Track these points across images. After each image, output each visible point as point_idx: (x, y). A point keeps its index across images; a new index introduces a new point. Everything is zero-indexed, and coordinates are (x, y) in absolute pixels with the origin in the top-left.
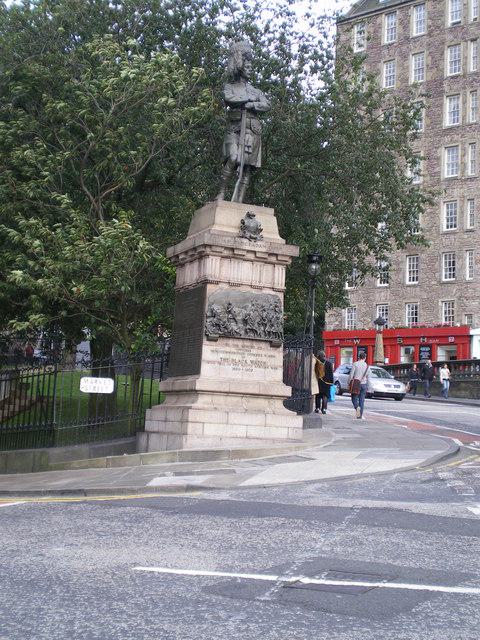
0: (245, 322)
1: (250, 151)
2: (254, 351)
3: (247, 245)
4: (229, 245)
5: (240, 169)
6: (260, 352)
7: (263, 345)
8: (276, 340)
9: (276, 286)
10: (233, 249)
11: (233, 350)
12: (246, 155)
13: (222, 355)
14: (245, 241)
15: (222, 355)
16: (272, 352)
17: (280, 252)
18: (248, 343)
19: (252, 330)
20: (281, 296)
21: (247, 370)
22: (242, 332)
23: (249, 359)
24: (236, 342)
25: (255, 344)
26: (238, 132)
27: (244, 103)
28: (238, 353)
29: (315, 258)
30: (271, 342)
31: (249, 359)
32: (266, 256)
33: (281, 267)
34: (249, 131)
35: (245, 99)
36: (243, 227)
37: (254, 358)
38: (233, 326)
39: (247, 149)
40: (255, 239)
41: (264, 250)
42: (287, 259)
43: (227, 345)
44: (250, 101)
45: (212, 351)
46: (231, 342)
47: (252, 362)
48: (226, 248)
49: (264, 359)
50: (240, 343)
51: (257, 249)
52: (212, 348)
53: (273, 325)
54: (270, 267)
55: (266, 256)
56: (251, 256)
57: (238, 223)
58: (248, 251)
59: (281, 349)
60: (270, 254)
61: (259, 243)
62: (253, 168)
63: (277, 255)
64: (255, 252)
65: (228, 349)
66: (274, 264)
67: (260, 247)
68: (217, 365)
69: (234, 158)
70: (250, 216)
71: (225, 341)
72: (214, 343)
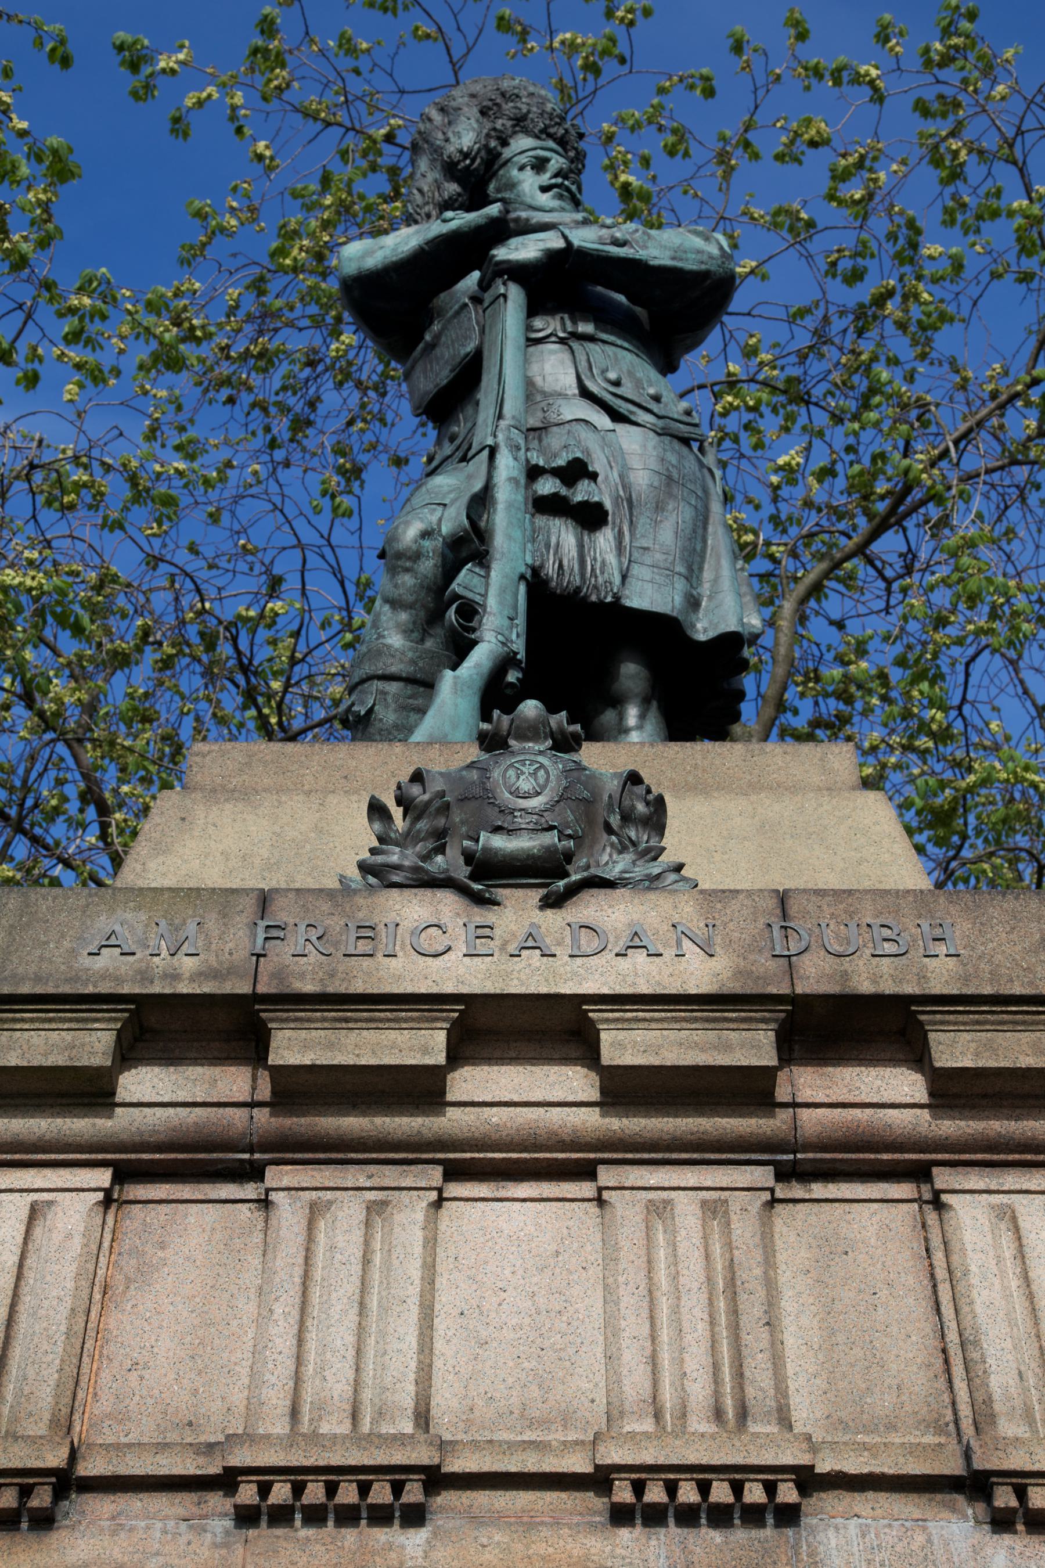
14: (412, 909)
17: (941, 975)
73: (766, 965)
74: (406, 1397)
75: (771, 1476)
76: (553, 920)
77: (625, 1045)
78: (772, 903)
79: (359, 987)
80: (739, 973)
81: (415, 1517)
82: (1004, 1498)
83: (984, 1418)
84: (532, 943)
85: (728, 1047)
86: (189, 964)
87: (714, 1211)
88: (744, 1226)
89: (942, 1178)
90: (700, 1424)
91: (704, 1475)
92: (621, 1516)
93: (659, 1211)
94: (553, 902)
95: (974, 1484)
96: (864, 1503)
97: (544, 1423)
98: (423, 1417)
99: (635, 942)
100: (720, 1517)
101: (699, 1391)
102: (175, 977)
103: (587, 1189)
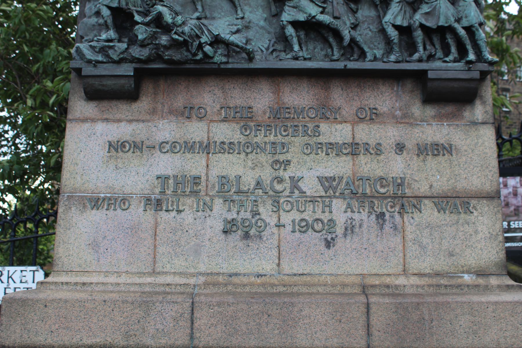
2: (338, 133)
6: (365, 133)
7: (384, 99)
8: (446, 68)
13: (166, 164)
15: (166, 164)
16: (436, 132)
18: (300, 97)
19: (310, 28)
21: (304, 227)
24: (239, 95)
28: (248, 148)
30: (419, 77)
31: (311, 171)
37: (339, 167)
43: (188, 113)
45: (117, 147)
46: (209, 96)
49: (396, 166)
50: (260, 98)
52: (122, 131)
65: (196, 131)
68: (137, 212)
71: (181, 96)
72: (123, 109)
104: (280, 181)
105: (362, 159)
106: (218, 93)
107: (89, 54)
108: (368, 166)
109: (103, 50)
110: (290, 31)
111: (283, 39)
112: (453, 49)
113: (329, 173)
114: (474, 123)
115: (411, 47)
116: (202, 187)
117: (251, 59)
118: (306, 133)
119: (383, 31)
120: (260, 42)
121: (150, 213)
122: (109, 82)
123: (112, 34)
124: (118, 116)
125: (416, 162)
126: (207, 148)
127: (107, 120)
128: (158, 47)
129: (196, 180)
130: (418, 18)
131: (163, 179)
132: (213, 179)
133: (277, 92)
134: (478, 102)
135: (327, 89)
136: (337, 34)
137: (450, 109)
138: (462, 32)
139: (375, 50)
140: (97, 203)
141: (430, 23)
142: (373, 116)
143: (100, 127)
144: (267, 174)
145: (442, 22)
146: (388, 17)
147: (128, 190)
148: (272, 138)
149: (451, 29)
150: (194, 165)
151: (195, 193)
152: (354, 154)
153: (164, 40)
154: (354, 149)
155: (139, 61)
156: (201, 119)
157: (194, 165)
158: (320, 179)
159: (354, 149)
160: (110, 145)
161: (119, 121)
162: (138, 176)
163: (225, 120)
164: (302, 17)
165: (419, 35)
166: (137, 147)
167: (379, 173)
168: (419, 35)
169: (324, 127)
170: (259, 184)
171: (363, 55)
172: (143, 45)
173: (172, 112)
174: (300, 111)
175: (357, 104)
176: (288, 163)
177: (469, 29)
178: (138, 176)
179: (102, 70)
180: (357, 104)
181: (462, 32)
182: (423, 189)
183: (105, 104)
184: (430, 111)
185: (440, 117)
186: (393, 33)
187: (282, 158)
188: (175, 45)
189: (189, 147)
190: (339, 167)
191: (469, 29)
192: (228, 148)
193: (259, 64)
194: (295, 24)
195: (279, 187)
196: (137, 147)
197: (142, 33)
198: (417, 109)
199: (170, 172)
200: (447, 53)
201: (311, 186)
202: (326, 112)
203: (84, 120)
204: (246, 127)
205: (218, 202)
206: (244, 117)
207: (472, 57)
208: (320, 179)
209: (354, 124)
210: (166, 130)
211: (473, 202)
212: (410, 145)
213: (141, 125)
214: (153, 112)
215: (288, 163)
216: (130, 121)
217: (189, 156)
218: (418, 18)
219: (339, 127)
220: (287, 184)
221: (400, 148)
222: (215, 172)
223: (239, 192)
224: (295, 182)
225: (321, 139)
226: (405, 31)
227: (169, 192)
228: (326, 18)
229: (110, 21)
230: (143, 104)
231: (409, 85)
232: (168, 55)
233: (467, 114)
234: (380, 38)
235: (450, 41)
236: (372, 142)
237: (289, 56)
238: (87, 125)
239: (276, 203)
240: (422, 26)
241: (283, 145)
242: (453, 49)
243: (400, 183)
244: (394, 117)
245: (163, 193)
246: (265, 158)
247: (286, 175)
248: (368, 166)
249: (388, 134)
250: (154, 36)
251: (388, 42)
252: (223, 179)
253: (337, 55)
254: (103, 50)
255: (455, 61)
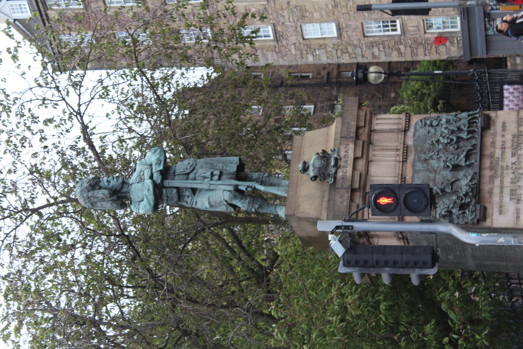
0: (456, 167)
1: (217, 172)
2: (498, 153)
3: (346, 171)
4: (347, 195)
5: (243, 186)
6: (499, 144)
7: (488, 140)
8: (479, 123)
9: (402, 126)
10: (353, 191)
11: (497, 182)
12: (224, 177)
13: (506, 198)
14: (340, 174)
15: (506, 198)
16: (498, 126)
17: (354, 123)
18: (487, 163)
19: (467, 157)
20: (416, 119)
22: (471, 172)
23: (509, 159)
25: (487, 151)
26: (194, 191)
27: (155, 185)
29: (360, 75)
31: (509, 159)
32: (360, 143)
33: (375, 121)
34: (192, 176)
35: (148, 183)
36: (321, 176)
37: (508, 152)
38: (464, 184)
39: (216, 178)
40: (336, 160)
41: (351, 146)
42: (362, 113)
43: (491, 193)
44: (151, 177)
45: (501, 212)
46: (486, 187)
47: (513, 155)
48: (352, 200)
49: (509, 137)
50: (487, 173)
51: (351, 156)
52: (496, 211)
53: (459, 129)
54: (375, 137)
55: (360, 143)
56: (361, 164)
57: (314, 184)
58: (354, 168)
59: (492, 114)
60: (357, 137)
61: (342, 154)
62: (241, 167)
63: (358, 128)
64: (355, 159)
65: (496, 191)
66: (371, 131)
67: (349, 151)
69: (227, 196)
70: (305, 169)
72: (489, 211)
73: (351, 139)
74: (393, 178)
75: (404, 147)
76: (343, 160)
77: (359, 154)
78: (342, 139)
79: (351, 178)
80: (352, 142)
81: (405, 178)
82: (407, 128)
83: (398, 129)
84: (346, 162)
85: (360, 145)
86: (346, 195)
87: (374, 150)
88: (376, 148)
89: (372, 129)
90: (398, 153)
91: (403, 153)
92: (406, 161)
93: (374, 155)
94: (341, 159)
95: (406, 131)
96: (406, 141)
97: (396, 167)
98: (395, 177)
99: (347, 152)
100: (407, 153)
101: (394, 153)
102: (348, 196)
103: (370, 163)
104: (512, 168)
105: (506, 146)
106: (484, 185)
107: (473, 216)
108: (508, 144)
109: (472, 212)
110: (468, 163)
111: (469, 166)
112: (475, 120)
113: (510, 155)
114: (496, 116)
115: (473, 132)
116: (514, 188)
117: (475, 173)
118: (498, 161)
119: (468, 139)
120: (471, 172)
121: (521, 202)
122: (482, 211)
123: (467, 211)
124: (491, 212)
125: (507, 132)
126: (502, 187)
127: (492, 216)
128: (472, 196)
129: (511, 190)
130: (465, 129)
131: (511, 199)
132: (512, 185)
133: (485, 169)
134: (490, 115)
135: (485, 155)
136: (469, 151)
137: (492, 123)
138: (470, 117)
139: (474, 142)
140: (518, 217)
141: (467, 126)
142: (493, 144)
143: (494, 217)
144: (510, 171)
145: (467, 122)
146: (465, 137)
147: (514, 208)
148: (499, 170)
149: (469, 120)
150: (507, 191)
151: (515, 190)
152: (505, 148)
153: (470, 194)
154: (503, 148)
155: (476, 202)
156: (493, 189)
157: (507, 191)
158: (512, 157)
159: (503, 148)
160: (500, 214)
161: (493, 212)
162: (510, 206)
163: (493, 183)
164: (464, 159)
165: (470, 129)
166: (501, 206)
167: (511, 141)
168: (470, 129)
169: (496, 156)
170: (513, 173)
171: (475, 145)
172: (471, 201)
173: (490, 197)
174: (491, 163)
175: (490, 147)
176: (507, 166)
177: (469, 116)
178: (510, 206)
179: (478, 214)
180: (490, 147)
181: (470, 117)
182: (515, 130)
183: (487, 216)
184: (492, 128)
185: (494, 125)
186: (469, 136)
187: (505, 167)
188: (472, 191)
189: (501, 192)
190: (508, 152)
191: (469, 116)
192: (502, 182)
193: (478, 171)
194: (466, 161)
195: (514, 168)
196: (501, 206)
197: (468, 200)
198: (492, 131)
199: (509, 197)
200: (476, 122)
201: (514, 159)
202: (492, 156)
203: (492, 222)
204: (496, 177)
205: (519, 184)
206: (492, 178)
207: (478, 115)
208: (512, 157)
209: (495, 148)
210: (496, 199)
211: (520, 117)
212: (502, 133)
213: (494, 206)
214: (490, 203)
215: (507, 166)
216: (493, 209)
217: (504, 192)
218: (465, 129)
219: (496, 152)
220: (513, 166)
221: (503, 136)
222: (509, 185)
223: (515, 178)
224: (513, 164)
225: (500, 156)
226: (469, 132)
227: (515, 197)
228: (464, 153)
229: (463, 211)
230: (488, 205)
231: (484, 133)
232: (475, 194)
233: (493, 118)
234: (470, 140)
235: (472, 121)
236: (501, 143)
237: (475, 163)
238: (494, 221)
239: (519, 169)
240: (468, 127)
241: (501, 167)
242: (475, 120)
243: (514, 136)
244: (494, 137)
245: (515, 199)
246: (505, 172)
247: (510, 166)
248: (508, 144)
249: (499, 140)
250: (469, 197)
251: (471, 138)
252: (512, 183)
253: (475, 151)
254: (472, 212)
255: (478, 119)
